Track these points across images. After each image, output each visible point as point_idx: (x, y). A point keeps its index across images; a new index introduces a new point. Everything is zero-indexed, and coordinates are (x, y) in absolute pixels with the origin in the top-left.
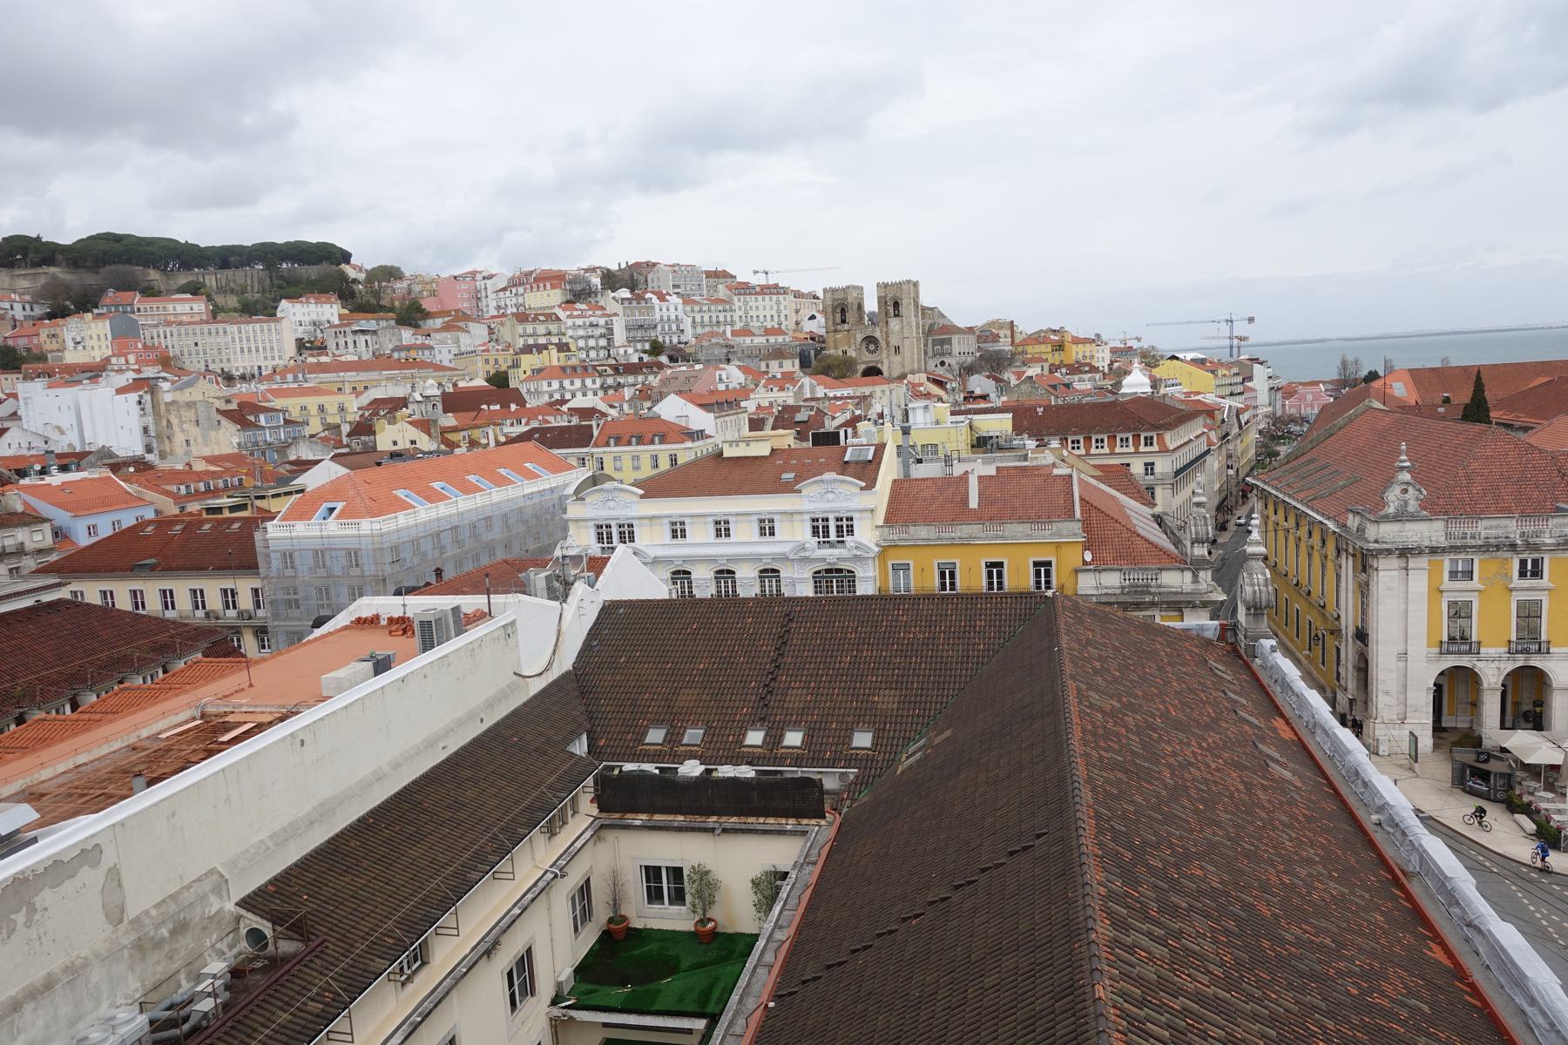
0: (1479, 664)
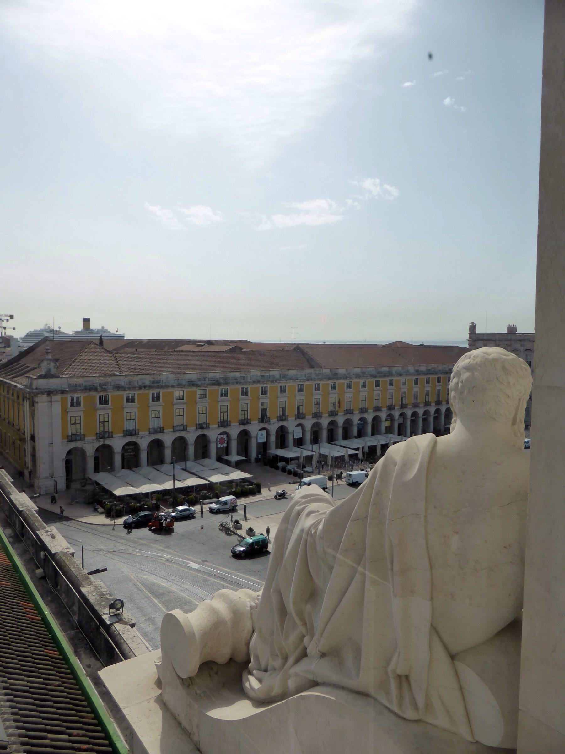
0: (85, 445)
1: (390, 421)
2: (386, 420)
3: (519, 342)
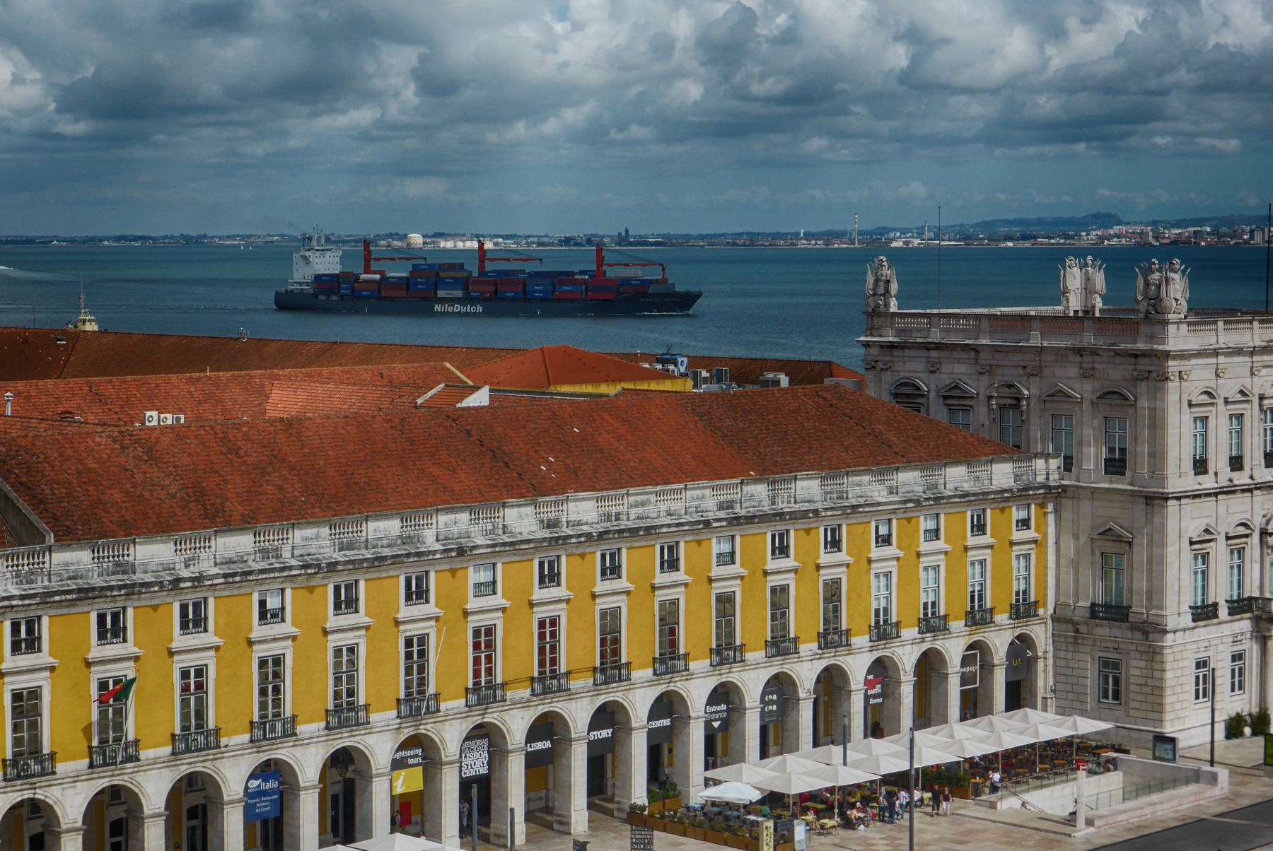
1: (421, 768)
2: (398, 765)
3: (1072, 358)
